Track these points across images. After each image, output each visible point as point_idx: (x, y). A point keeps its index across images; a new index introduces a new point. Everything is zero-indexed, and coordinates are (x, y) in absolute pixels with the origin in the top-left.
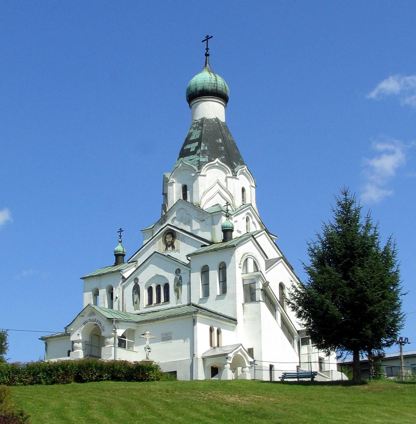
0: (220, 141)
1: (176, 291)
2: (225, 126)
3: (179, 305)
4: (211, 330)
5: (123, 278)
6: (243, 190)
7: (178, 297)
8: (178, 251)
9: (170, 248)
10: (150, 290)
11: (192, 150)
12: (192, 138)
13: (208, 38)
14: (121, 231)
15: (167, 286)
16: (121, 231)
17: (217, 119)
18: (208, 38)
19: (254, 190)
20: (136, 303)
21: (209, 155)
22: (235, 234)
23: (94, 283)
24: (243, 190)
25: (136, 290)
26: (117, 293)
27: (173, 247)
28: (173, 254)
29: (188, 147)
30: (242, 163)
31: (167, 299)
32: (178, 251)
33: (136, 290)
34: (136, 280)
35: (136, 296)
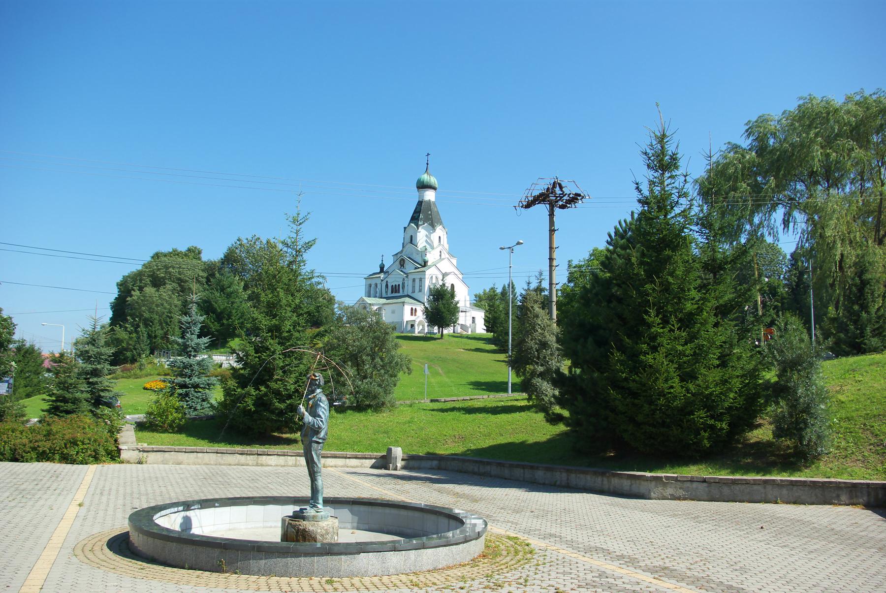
0: (430, 212)
1: (403, 288)
2: (434, 203)
4: (412, 309)
6: (440, 237)
13: (428, 155)
15: (399, 285)
18: (428, 155)
19: (446, 236)
20: (386, 292)
22: (429, 264)
23: (370, 281)
24: (440, 237)
25: (387, 286)
26: (379, 286)
30: (441, 223)
31: (399, 292)
33: (387, 286)
34: (387, 281)
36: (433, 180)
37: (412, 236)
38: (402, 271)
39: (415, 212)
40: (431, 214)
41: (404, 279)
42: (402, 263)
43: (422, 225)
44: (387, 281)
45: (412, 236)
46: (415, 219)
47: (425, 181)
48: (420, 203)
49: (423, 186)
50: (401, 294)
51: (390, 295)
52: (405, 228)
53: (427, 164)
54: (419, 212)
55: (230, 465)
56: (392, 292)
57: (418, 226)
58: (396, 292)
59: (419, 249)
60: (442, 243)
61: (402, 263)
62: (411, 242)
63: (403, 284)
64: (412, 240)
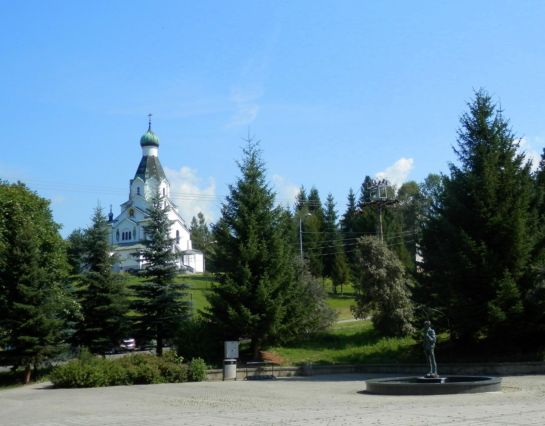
0: (154, 167)
2: (157, 158)
3: (135, 241)
5: (113, 228)
6: (164, 189)
7: (135, 238)
8: (135, 218)
9: (132, 216)
10: (123, 233)
11: (142, 171)
12: (142, 165)
13: (150, 115)
14: (111, 206)
15: (130, 233)
16: (111, 206)
17: (153, 156)
18: (150, 115)
19: (168, 188)
20: (118, 239)
21: (149, 174)
24: (164, 189)
25: (118, 233)
27: (133, 216)
28: (133, 219)
29: (140, 169)
31: (130, 238)
32: (135, 218)
33: (118, 233)
34: (118, 229)
35: (118, 236)
36: (156, 138)
37: (139, 188)
38: (131, 220)
39: (140, 166)
40: (155, 169)
41: (135, 228)
42: (132, 214)
43: (148, 178)
44: (118, 229)
45: (139, 188)
46: (141, 172)
47: (149, 138)
48: (145, 158)
49: (147, 143)
50: (132, 240)
51: (121, 241)
52: (132, 181)
53: (150, 123)
54: (145, 167)
55: (317, 419)
56: (123, 239)
57: (145, 180)
58: (127, 239)
59: (146, 199)
60: (166, 194)
61: (132, 214)
62: (139, 194)
63: (135, 231)
64: (139, 192)
